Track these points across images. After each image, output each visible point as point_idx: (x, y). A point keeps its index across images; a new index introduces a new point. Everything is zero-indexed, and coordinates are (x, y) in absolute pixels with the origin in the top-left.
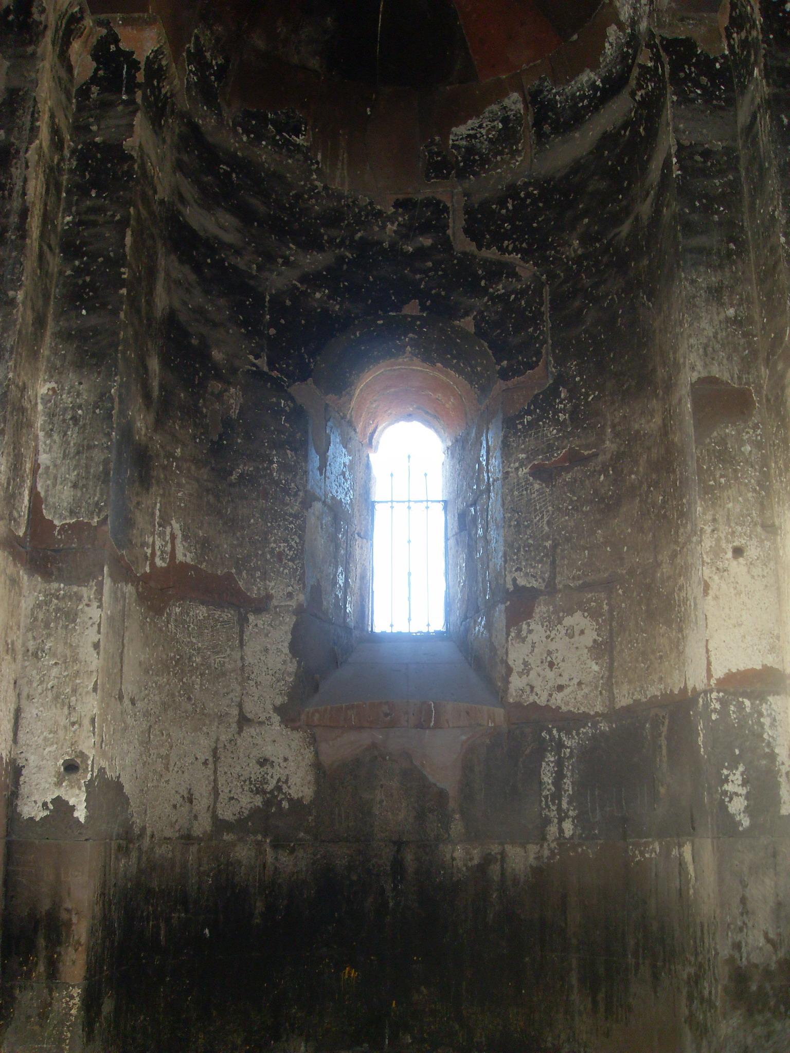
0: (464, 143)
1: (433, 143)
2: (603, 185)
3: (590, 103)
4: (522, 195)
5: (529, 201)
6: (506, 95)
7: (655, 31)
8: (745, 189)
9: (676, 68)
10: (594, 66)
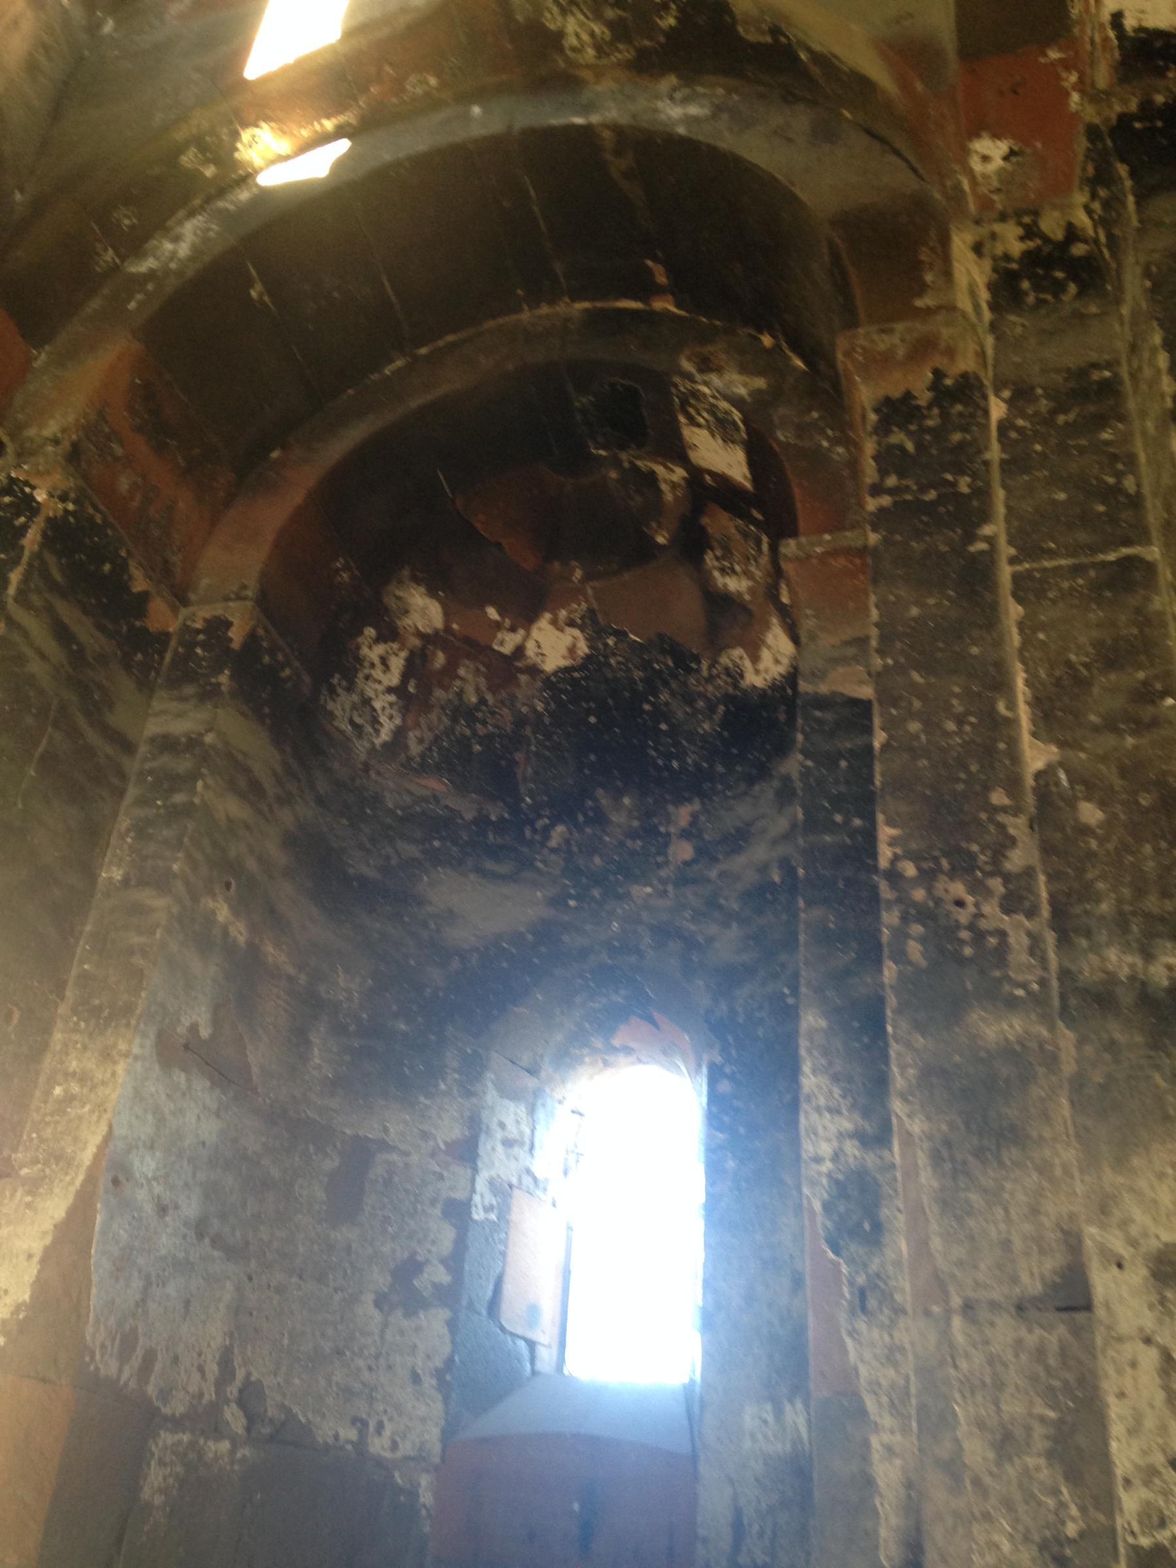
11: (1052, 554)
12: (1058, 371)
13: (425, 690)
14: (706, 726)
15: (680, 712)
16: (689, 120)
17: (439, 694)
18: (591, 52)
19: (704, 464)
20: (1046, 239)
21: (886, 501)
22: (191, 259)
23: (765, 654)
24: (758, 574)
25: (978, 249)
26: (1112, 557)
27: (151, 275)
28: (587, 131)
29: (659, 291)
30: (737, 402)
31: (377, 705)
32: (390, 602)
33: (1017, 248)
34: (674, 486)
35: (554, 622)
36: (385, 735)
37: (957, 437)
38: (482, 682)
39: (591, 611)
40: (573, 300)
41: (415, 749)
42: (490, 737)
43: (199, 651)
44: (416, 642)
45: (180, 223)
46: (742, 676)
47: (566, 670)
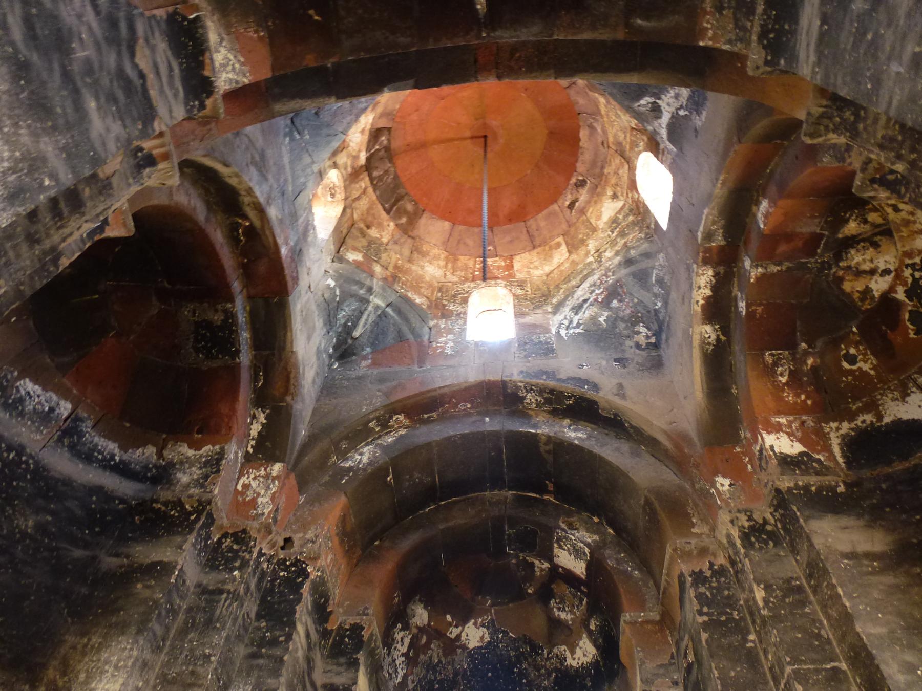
0: (23, 392)
1: (12, 372)
2: (79, 512)
3: (102, 461)
4: (24, 458)
5: (23, 466)
6: (66, 399)
7: (213, 504)
8: (181, 617)
9: (201, 528)
10: (124, 448)
11: (805, 662)
12: (779, 579)
13: (417, 655)
14: (546, 682)
15: (533, 674)
16: (578, 438)
17: (422, 657)
18: (534, 405)
19: (560, 564)
20: (757, 523)
21: (706, 618)
22: (369, 464)
23: (578, 650)
24: (578, 613)
25: (732, 522)
26: (828, 667)
27: (350, 469)
28: (535, 435)
29: (548, 492)
30: (588, 545)
31: (398, 662)
32: (409, 611)
33: (746, 524)
34: (542, 570)
35: (475, 624)
36: (399, 679)
37: (726, 592)
38: (441, 651)
39: (492, 620)
40: (510, 489)
41: (411, 686)
42: (441, 682)
43: (347, 640)
44: (415, 630)
45: (362, 447)
46: (565, 659)
47: (479, 648)
